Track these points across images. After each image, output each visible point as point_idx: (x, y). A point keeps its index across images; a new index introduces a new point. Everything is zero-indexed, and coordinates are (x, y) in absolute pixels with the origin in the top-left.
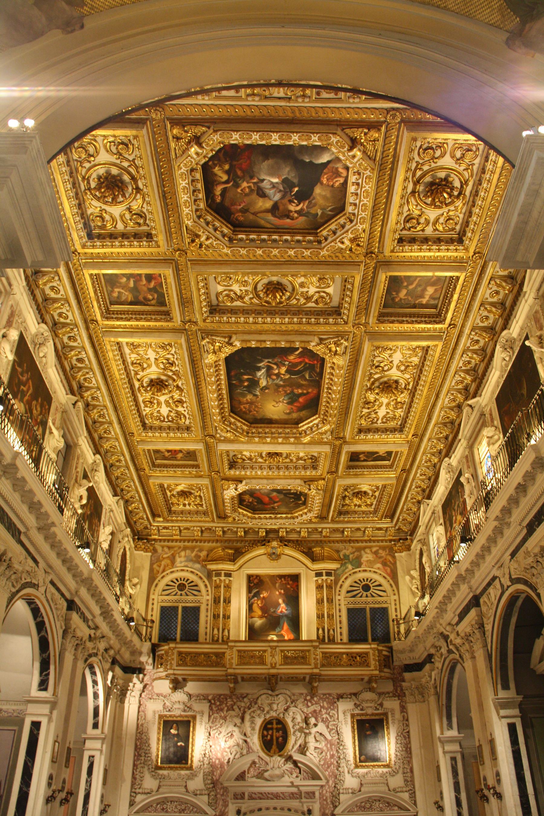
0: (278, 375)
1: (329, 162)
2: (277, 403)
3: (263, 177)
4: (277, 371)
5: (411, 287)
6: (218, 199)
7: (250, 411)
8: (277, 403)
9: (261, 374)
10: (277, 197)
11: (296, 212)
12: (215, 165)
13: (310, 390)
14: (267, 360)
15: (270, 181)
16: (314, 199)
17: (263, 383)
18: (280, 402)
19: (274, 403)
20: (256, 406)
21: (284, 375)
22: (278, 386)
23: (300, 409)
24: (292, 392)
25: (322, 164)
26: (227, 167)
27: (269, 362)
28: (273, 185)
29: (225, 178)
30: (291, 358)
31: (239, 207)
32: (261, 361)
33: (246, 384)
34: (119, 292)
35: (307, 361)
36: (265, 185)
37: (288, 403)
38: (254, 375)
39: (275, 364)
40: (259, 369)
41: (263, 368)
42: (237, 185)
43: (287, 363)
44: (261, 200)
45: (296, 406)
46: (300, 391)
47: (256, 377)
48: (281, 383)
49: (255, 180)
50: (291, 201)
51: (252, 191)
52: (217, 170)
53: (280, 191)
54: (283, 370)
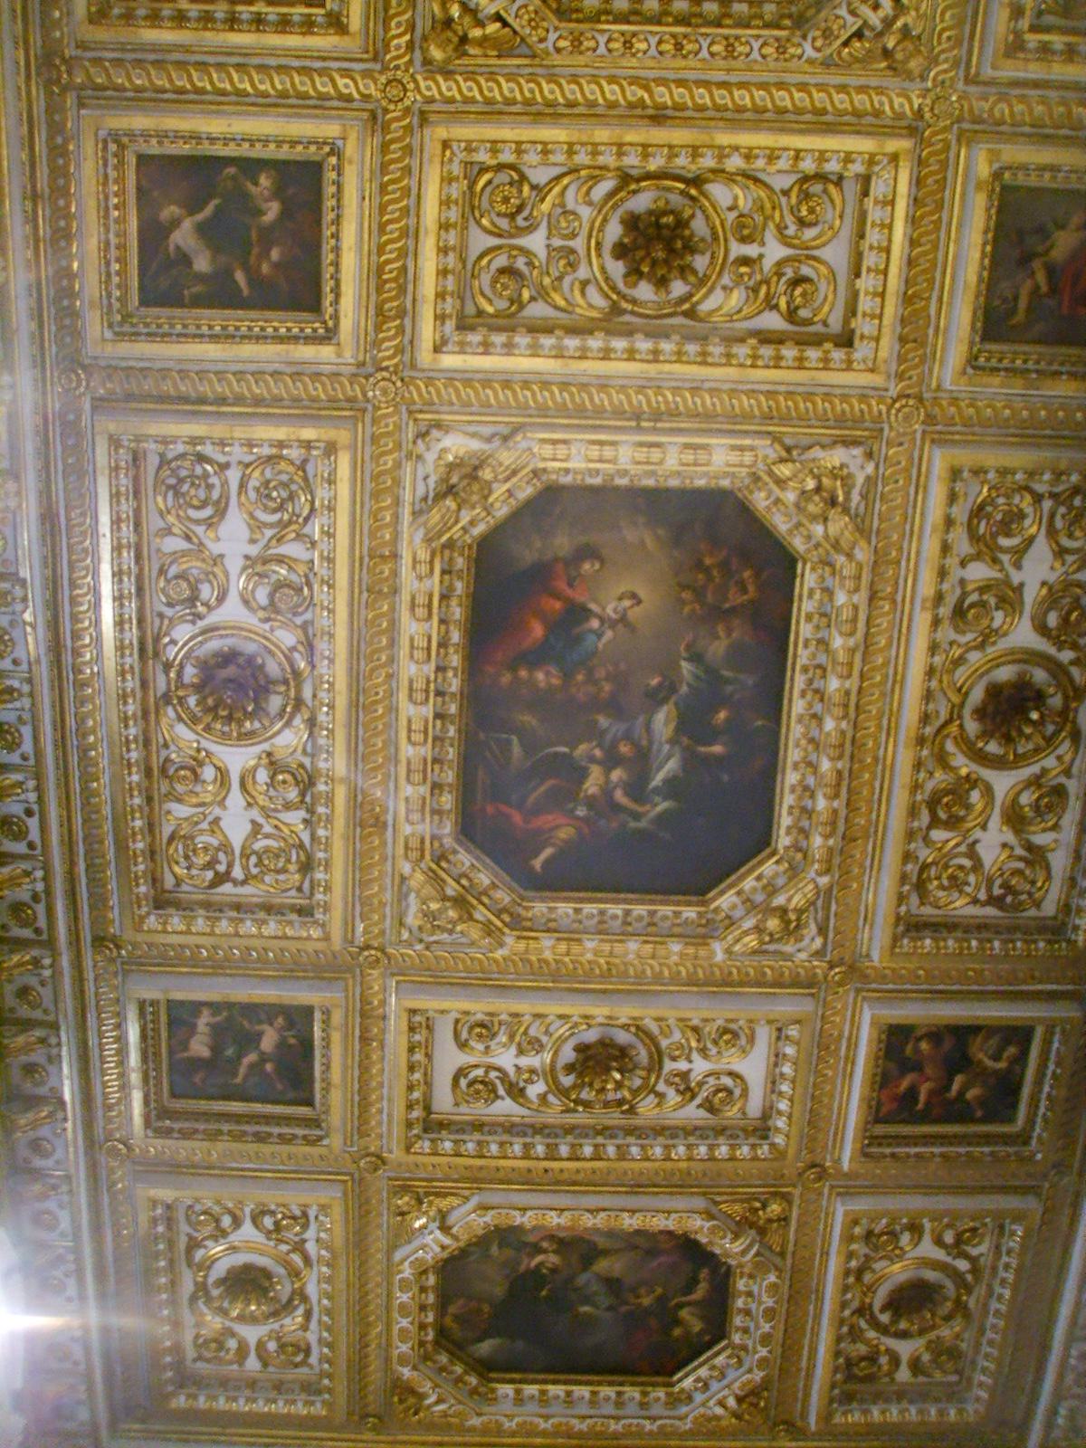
0: (612, 761)
1: (480, 1340)
2: (623, 619)
3: (608, 1315)
4: (616, 775)
5: (252, 1057)
6: (704, 1273)
7: (724, 566)
8: (623, 619)
9: (668, 768)
10: (582, 1279)
11: (545, 1251)
12: (700, 1334)
13: (506, 678)
14: (643, 824)
15: (597, 1307)
16: (507, 1276)
17: (663, 721)
18: (613, 624)
19: (635, 614)
20: (699, 594)
21: (592, 759)
22: (615, 707)
23: (541, 576)
24: (567, 676)
25: (491, 1336)
26: (677, 1332)
27: (637, 816)
28: (587, 1300)
29: (684, 1313)
30: (565, 833)
31: (663, 1259)
32: (661, 819)
33: (722, 715)
34: (996, 1058)
35: (517, 818)
36: (605, 1300)
37: (585, 613)
38: (692, 761)
39: (616, 808)
40: (672, 788)
41: (656, 790)
42: (662, 1300)
43: (581, 812)
44: (616, 1274)
45: (557, 596)
46: (540, 676)
47: (686, 749)
48: (603, 721)
49: (624, 1309)
50: (554, 1271)
51: (634, 1290)
52: (697, 1326)
53: (576, 1289)
54: (592, 785)
